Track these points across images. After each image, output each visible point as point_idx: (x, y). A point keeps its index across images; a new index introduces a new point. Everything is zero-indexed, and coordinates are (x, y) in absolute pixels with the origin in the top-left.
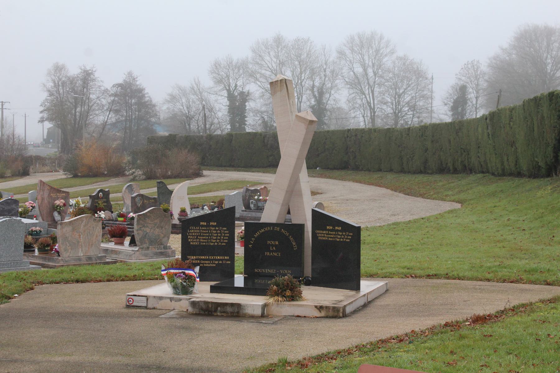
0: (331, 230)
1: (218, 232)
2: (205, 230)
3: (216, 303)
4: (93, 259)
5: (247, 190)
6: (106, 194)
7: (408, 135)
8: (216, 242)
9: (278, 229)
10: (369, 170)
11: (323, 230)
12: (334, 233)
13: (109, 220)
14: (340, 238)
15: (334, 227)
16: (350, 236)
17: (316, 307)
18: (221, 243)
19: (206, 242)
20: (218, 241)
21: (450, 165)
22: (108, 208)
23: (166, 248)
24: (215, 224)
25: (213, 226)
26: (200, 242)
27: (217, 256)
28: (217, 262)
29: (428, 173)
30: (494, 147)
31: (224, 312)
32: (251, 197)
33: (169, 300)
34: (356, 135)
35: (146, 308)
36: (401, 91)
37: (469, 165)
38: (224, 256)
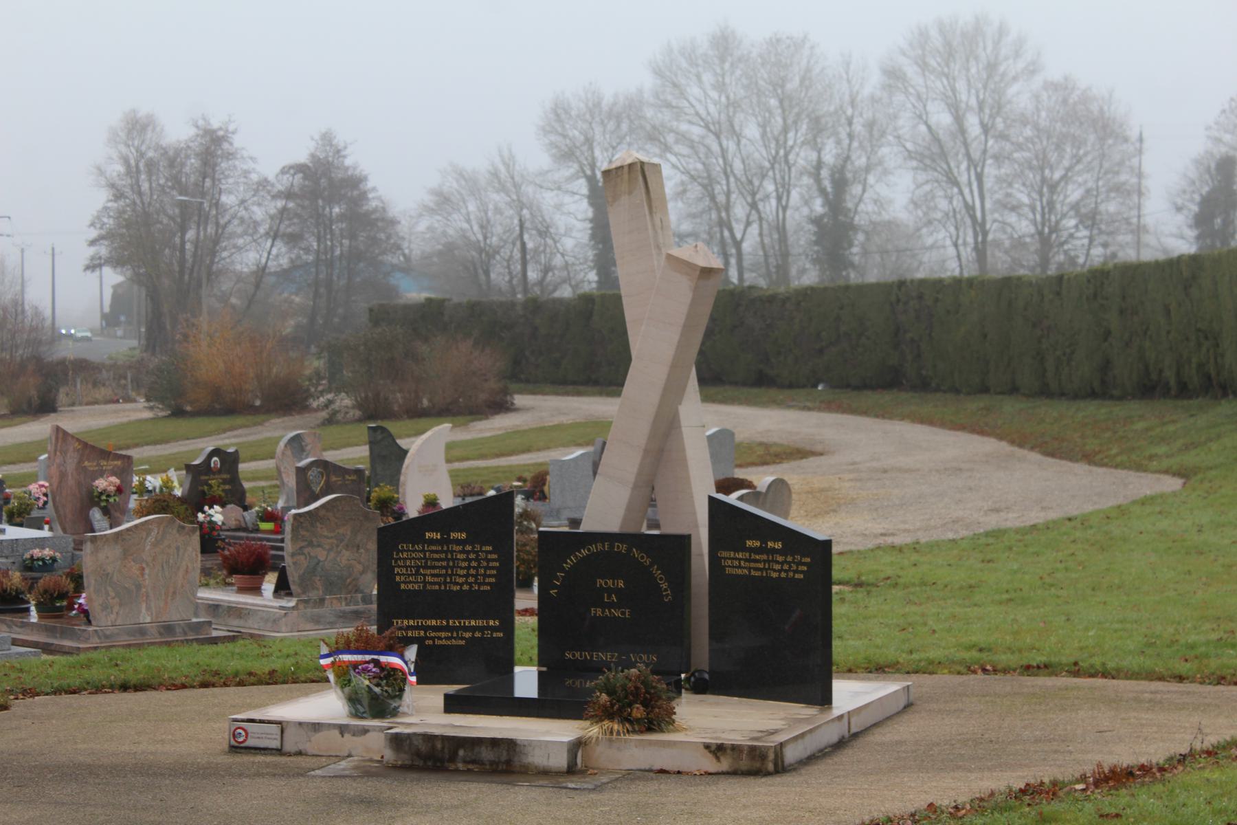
1: (472, 556)
2: (436, 552)
3: (454, 737)
4: (178, 630)
6: (230, 461)
7: (1058, 294)
8: (466, 582)
9: (623, 548)
10: (957, 391)
11: (736, 550)
12: (765, 557)
13: (238, 529)
14: (780, 571)
16: (804, 564)
17: (707, 746)
18: (480, 584)
19: (439, 584)
20: (471, 580)
21: (1170, 375)
22: (235, 496)
24: (464, 535)
26: (425, 583)
27: (470, 618)
28: (468, 635)
29: (1112, 397)
31: (473, 762)
33: (336, 732)
34: (920, 297)
35: (279, 751)
36: (1057, 175)
37: (1218, 374)
38: (487, 618)
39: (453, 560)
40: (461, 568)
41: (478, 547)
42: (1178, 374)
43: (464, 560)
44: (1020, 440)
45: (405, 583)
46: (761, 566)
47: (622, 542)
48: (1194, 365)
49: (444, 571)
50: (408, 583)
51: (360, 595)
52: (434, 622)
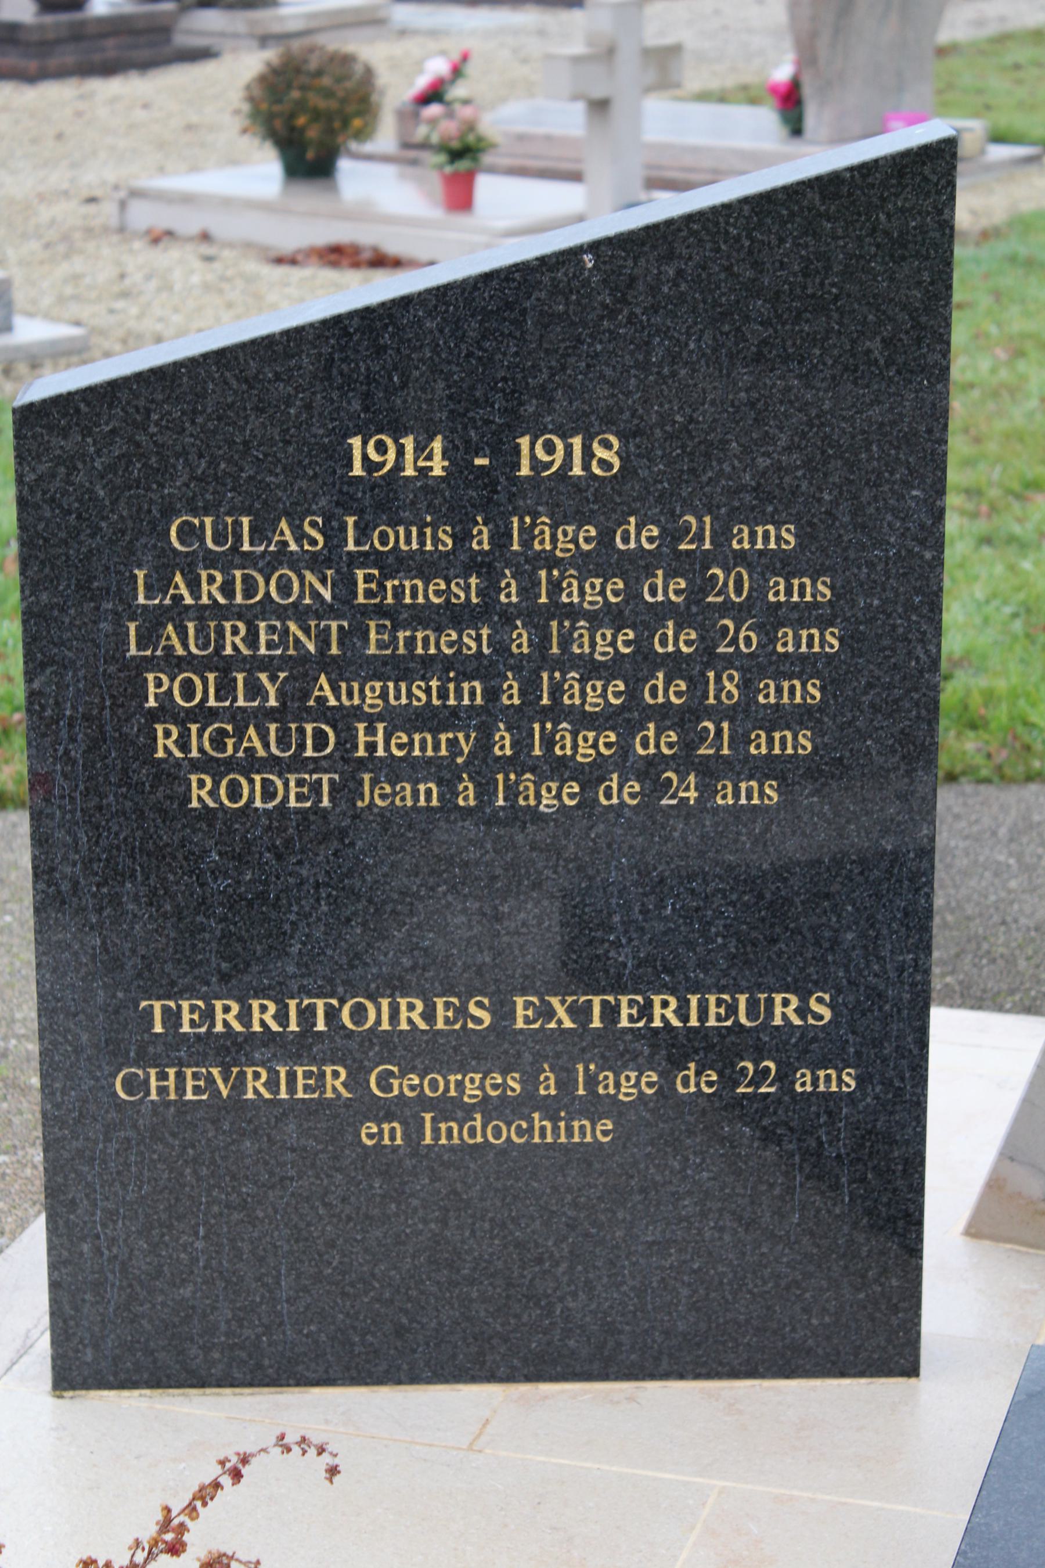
2: (426, 567)
18: (710, 772)
19: (446, 774)
20: (654, 741)
24: (608, 454)
25: (568, 498)
26: (349, 767)
28: (632, 1085)
40: (591, 669)
41: (699, 529)
43: (613, 617)
45: (205, 764)
50: (245, 781)
52: (411, 1013)
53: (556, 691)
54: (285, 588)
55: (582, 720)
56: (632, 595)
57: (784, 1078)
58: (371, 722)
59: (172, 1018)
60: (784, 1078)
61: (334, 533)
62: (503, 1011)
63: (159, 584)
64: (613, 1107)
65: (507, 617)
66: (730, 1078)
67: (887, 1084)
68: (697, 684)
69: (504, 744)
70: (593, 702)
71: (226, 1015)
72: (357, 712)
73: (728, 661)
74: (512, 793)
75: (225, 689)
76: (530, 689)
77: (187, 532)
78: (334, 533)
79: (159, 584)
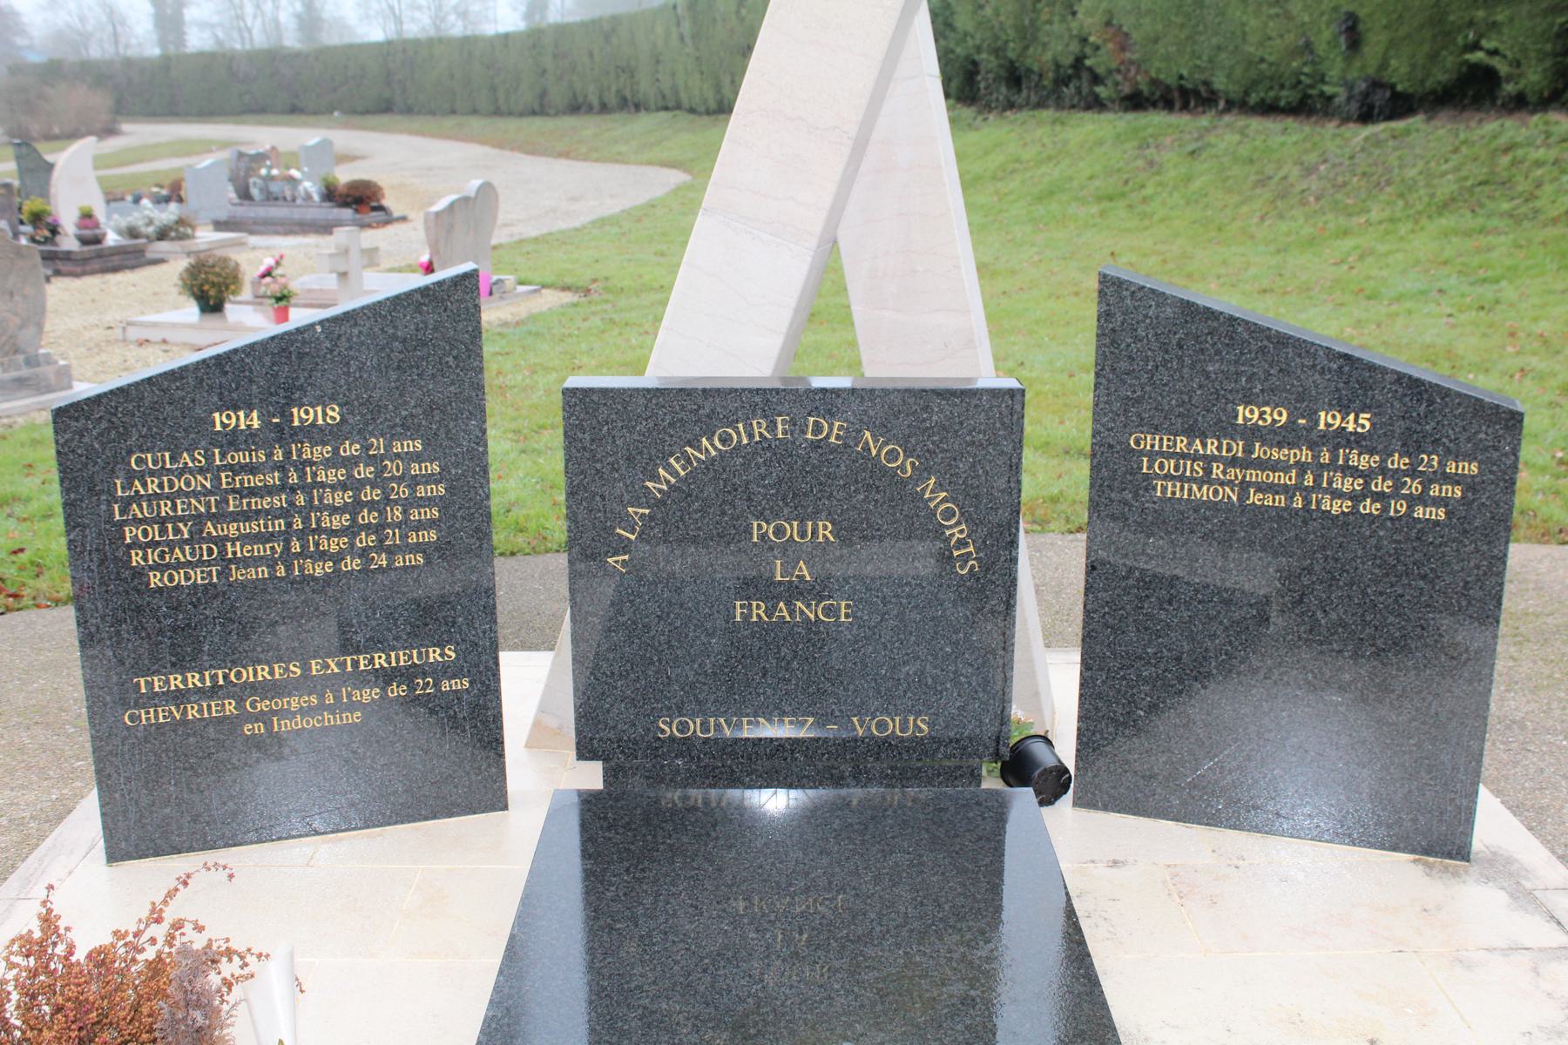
0: (1285, 437)
1: (364, 472)
2: (252, 469)
5: (241, 155)
9: (834, 430)
10: (432, 113)
11: (1191, 432)
12: (1305, 455)
14: (1356, 498)
15: (1304, 404)
20: (365, 540)
23: (32, 362)
24: (334, 413)
26: (225, 563)
28: (369, 694)
29: (548, 114)
30: (697, 59)
32: (250, 171)
34: (404, 51)
39: (307, 489)
40: (334, 510)
41: (378, 444)
42: (600, 98)
44: (500, 145)
45: (156, 567)
46: (1289, 479)
47: (830, 414)
48: (614, 88)
49: (280, 524)
50: (177, 572)
51: (20, 358)
52: (263, 673)
53: (318, 521)
54: (188, 484)
55: (332, 533)
56: (350, 476)
57: (437, 685)
58: (233, 541)
59: (150, 685)
60: (437, 685)
61: (209, 457)
62: (306, 667)
63: (128, 485)
64: (360, 705)
65: (293, 490)
66: (412, 688)
67: (483, 683)
68: (382, 513)
69: (296, 547)
70: (336, 525)
71: (176, 681)
72: (227, 538)
73: (396, 502)
74: (302, 569)
75: (163, 531)
76: (306, 520)
77: (139, 461)
78: (209, 457)
79: (128, 485)
